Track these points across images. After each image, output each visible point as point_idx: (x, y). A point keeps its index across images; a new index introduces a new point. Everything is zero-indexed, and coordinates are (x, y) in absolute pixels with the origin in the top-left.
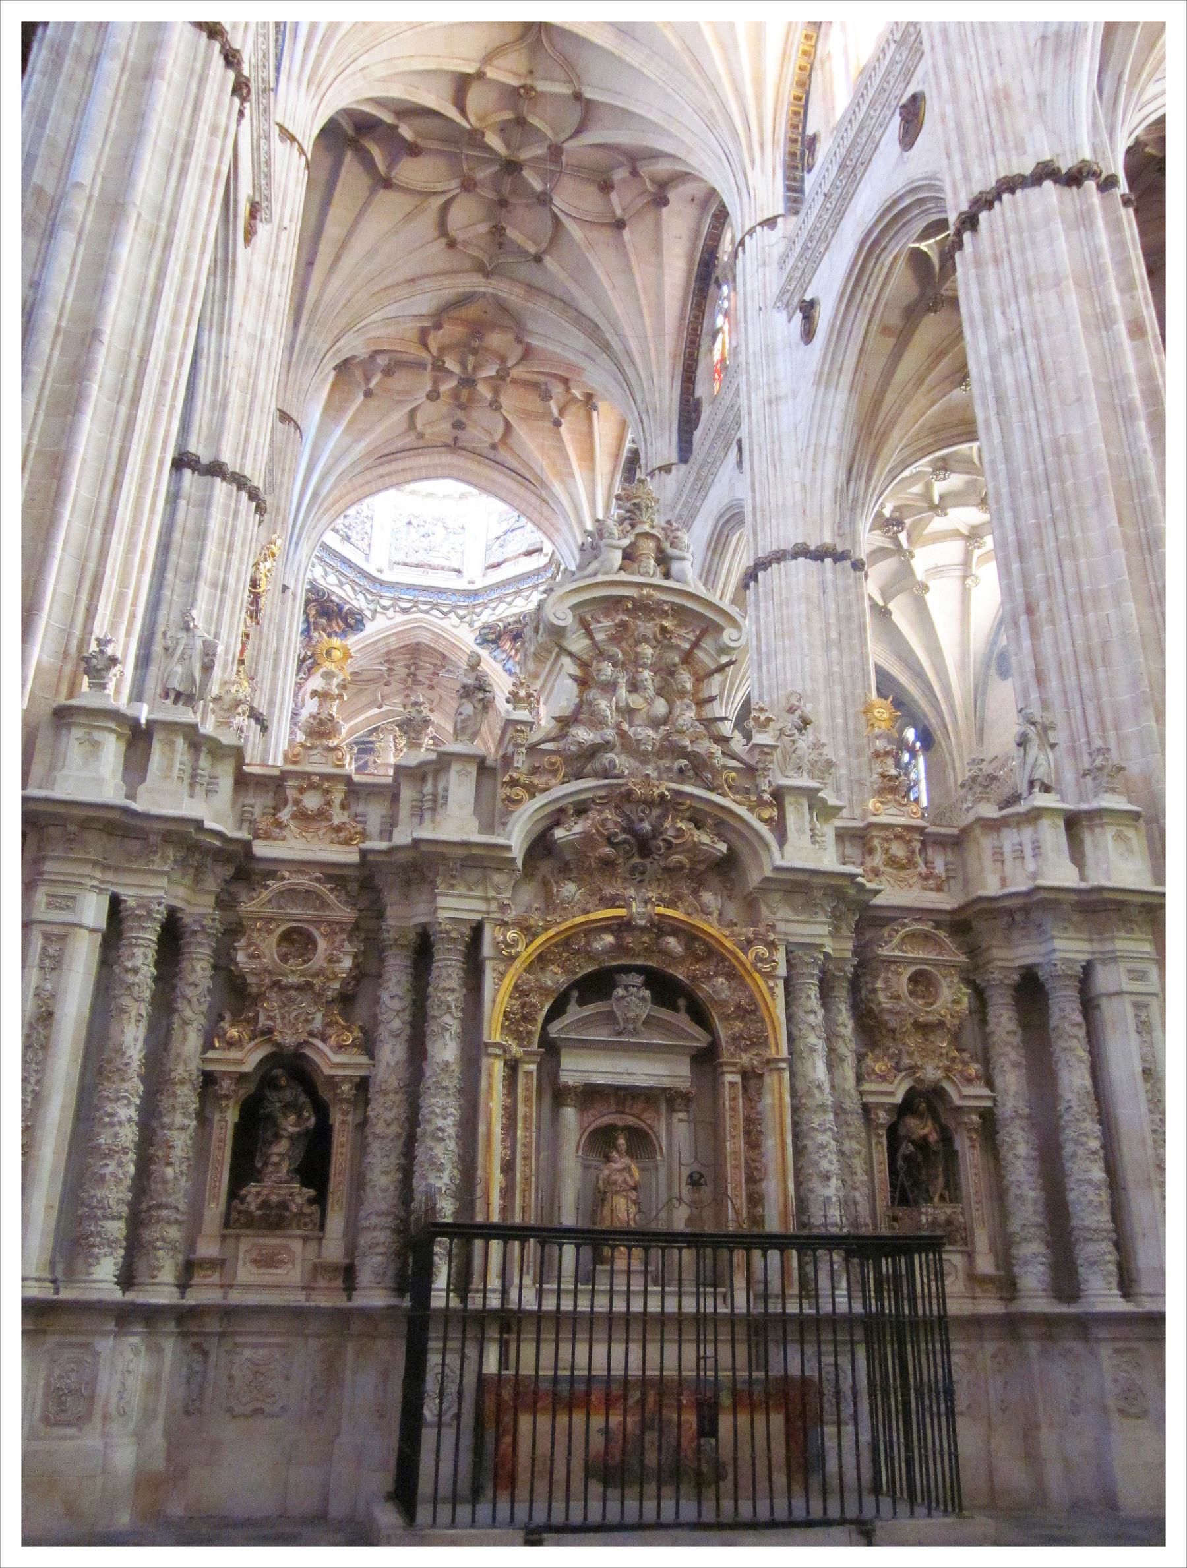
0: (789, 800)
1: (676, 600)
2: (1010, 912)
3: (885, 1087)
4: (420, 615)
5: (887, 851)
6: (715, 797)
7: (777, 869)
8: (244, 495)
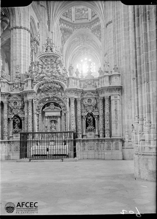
0: (70, 79)
1: (52, 55)
2: (101, 90)
3: (85, 113)
4: (82, 29)
5: (88, 83)
6: (58, 81)
7: (66, 89)
8: (26, 31)
